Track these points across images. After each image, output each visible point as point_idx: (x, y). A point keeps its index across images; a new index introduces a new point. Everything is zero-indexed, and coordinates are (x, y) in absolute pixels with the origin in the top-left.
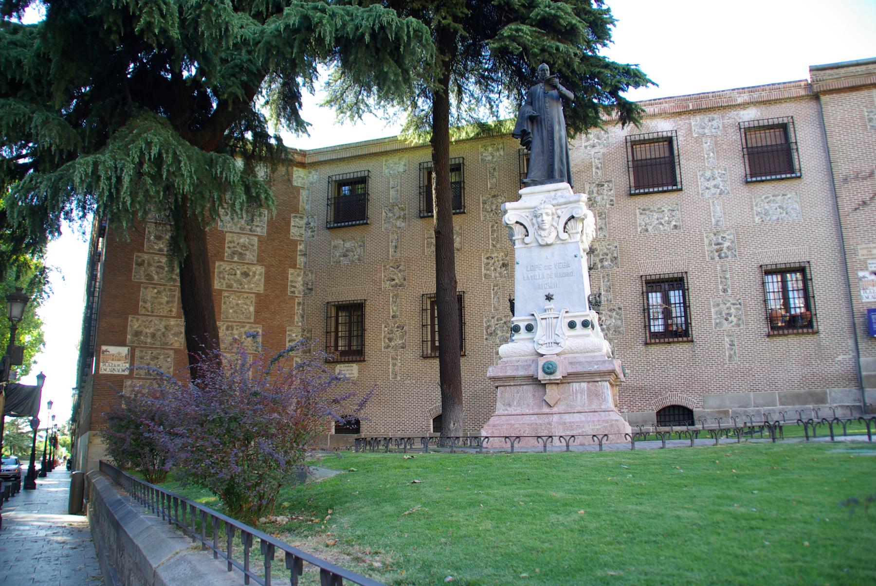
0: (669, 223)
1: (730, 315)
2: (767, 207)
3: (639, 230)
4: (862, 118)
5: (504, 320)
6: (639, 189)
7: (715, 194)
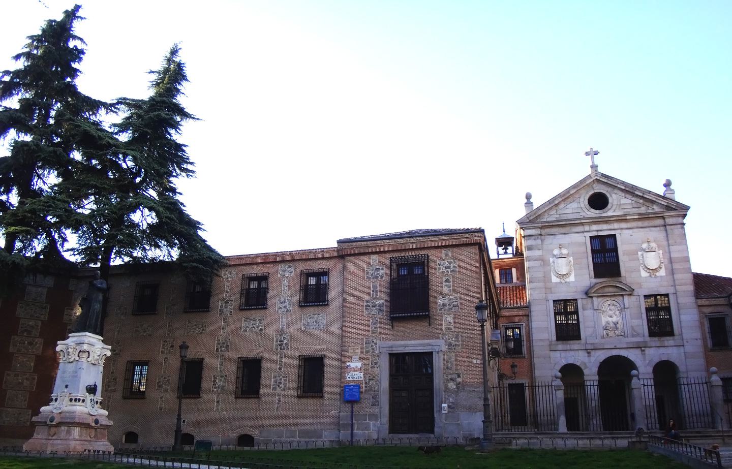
0: (258, 327)
2: (309, 321)
3: (242, 330)
4: (363, 271)
5: (168, 378)
7: (284, 312)
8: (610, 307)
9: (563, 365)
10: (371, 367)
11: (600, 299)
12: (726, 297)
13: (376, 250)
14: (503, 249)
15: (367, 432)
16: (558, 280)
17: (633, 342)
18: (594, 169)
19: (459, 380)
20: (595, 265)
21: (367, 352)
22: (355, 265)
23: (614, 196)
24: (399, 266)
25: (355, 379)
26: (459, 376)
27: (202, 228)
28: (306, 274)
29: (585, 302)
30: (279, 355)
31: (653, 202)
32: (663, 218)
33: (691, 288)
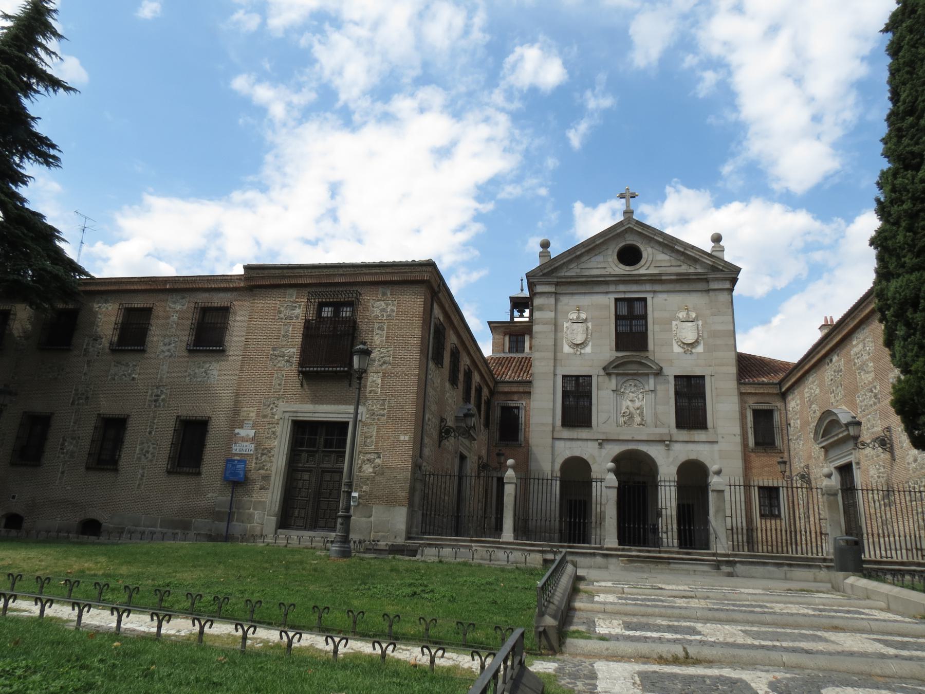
0: (130, 375)
1: (147, 452)
2: (196, 371)
3: (110, 377)
7: (166, 356)
8: (632, 387)
9: (566, 457)
10: (267, 438)
11: (619, 378)
13: (293, 281)
14: (518, 311)
15: (249, 525)
16: (571, 351)
18: (629, 215)
20: (618, 335)
21: (265, 416)
22: (266, 304)
23: (650, 250)
24: (321, 305)
25: (243, 453)
26: (379, 457)
27: (60, 238)
29: (601, 379)
30: (151, 415)
31: (695, 260)
32: (707, 280)
33: (733, 370)
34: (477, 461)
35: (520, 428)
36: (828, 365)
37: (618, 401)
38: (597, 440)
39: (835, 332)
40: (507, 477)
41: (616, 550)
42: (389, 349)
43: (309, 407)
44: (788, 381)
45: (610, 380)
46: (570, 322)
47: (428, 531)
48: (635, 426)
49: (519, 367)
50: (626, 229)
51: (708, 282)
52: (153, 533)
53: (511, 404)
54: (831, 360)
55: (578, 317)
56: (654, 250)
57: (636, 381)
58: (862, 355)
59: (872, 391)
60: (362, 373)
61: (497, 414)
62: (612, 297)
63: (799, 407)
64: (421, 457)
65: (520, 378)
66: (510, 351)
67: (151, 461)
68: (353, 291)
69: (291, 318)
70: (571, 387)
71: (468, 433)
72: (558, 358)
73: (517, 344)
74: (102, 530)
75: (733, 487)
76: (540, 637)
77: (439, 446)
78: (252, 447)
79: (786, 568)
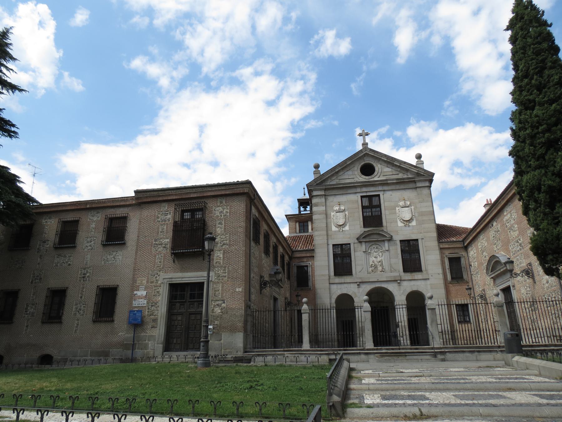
1: (80, 309)
2: (108, 257)
3: (54, 265)
4: (155, 216)
6: (61, 245)
7: (89, 249)
9: (339, 294)
10: (154, 296)
11: (367, 244)
12: (461, 241)
14: (303, 208)
15: (146, 351)
16: (337, 229)
17: (392, 276)
18: (365, 146)
19: (223, 305)
20: (364, 218)
21: (152, 282)
22: (149, 212)
23: (379, 166)
24: (183, 212)
28: (110, 218)
31: (407, 170)
32: (415, 182)
33: (435, 234)
34: (284, 301)
35: (309, 278)
36: (491, 228)
37: (368, 258)
38: (356, 282)
39: (493, 208)
40: (303, 310)
41: (373, 349)
42: (226, 236)
43: (180, 275)
44: (468, 239)
45: (361, 245)
46: (335, 212)
47: (257, 346)
48: (379, 272)
49: (306, 241)
50: (364, 154)
51: (415, 183)
52: (86, 360)
53: (303, 264)
54: (492, 225)
55: (340, 209)
56: (382, 166)
57: (377, 245)
58: (510, 221)
59: (518, 242)
60: (211, 252)
61: (294, 270)
62: (359, 195)
63: (475, 255)
64: (250, 301)
65: (307, 248)
66: (300, 232)
67: (83, 315)
68: (202, 202)
69: (165, 221)
70: (339, 251)
71: (277, 284)
72: (329, 234)
73: (304, 227)
74: (53, 361)
75: (440, 306)
76: (331, 409)
77: (261, 293)
78: (145, 302)
79: (476, 353)
